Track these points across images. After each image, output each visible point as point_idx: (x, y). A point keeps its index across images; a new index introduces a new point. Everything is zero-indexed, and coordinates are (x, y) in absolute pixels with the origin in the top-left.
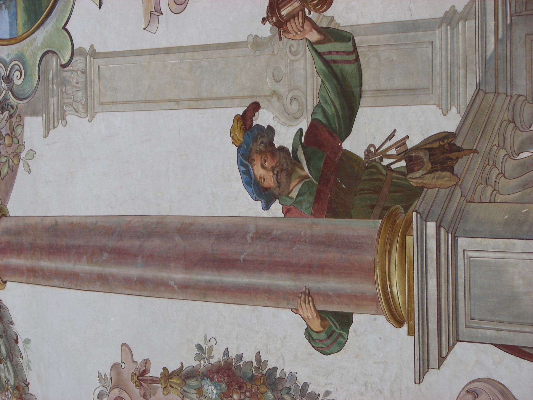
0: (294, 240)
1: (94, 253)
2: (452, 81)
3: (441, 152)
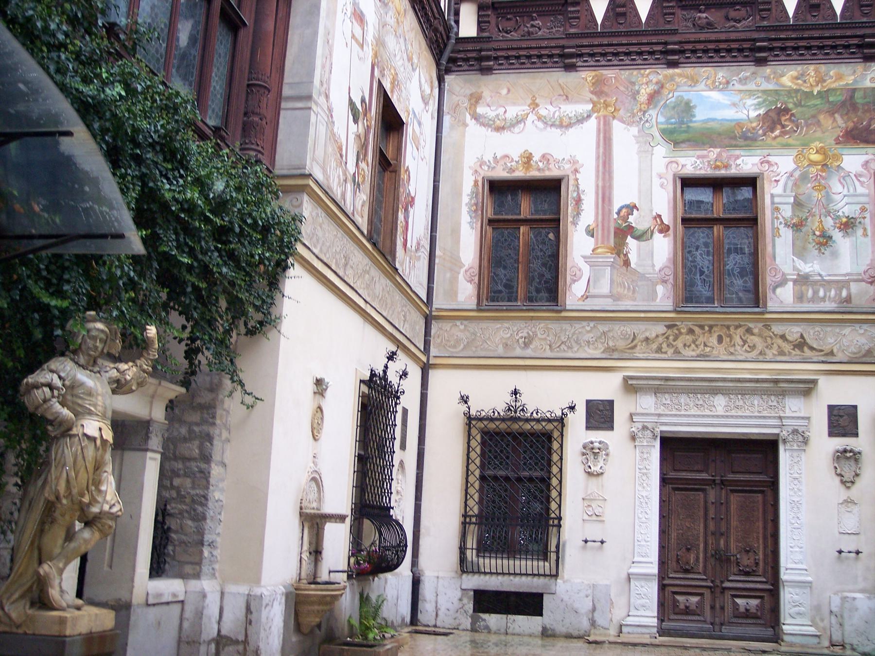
0: (609, 221)
1: (604, 154)
3: (627, 263)
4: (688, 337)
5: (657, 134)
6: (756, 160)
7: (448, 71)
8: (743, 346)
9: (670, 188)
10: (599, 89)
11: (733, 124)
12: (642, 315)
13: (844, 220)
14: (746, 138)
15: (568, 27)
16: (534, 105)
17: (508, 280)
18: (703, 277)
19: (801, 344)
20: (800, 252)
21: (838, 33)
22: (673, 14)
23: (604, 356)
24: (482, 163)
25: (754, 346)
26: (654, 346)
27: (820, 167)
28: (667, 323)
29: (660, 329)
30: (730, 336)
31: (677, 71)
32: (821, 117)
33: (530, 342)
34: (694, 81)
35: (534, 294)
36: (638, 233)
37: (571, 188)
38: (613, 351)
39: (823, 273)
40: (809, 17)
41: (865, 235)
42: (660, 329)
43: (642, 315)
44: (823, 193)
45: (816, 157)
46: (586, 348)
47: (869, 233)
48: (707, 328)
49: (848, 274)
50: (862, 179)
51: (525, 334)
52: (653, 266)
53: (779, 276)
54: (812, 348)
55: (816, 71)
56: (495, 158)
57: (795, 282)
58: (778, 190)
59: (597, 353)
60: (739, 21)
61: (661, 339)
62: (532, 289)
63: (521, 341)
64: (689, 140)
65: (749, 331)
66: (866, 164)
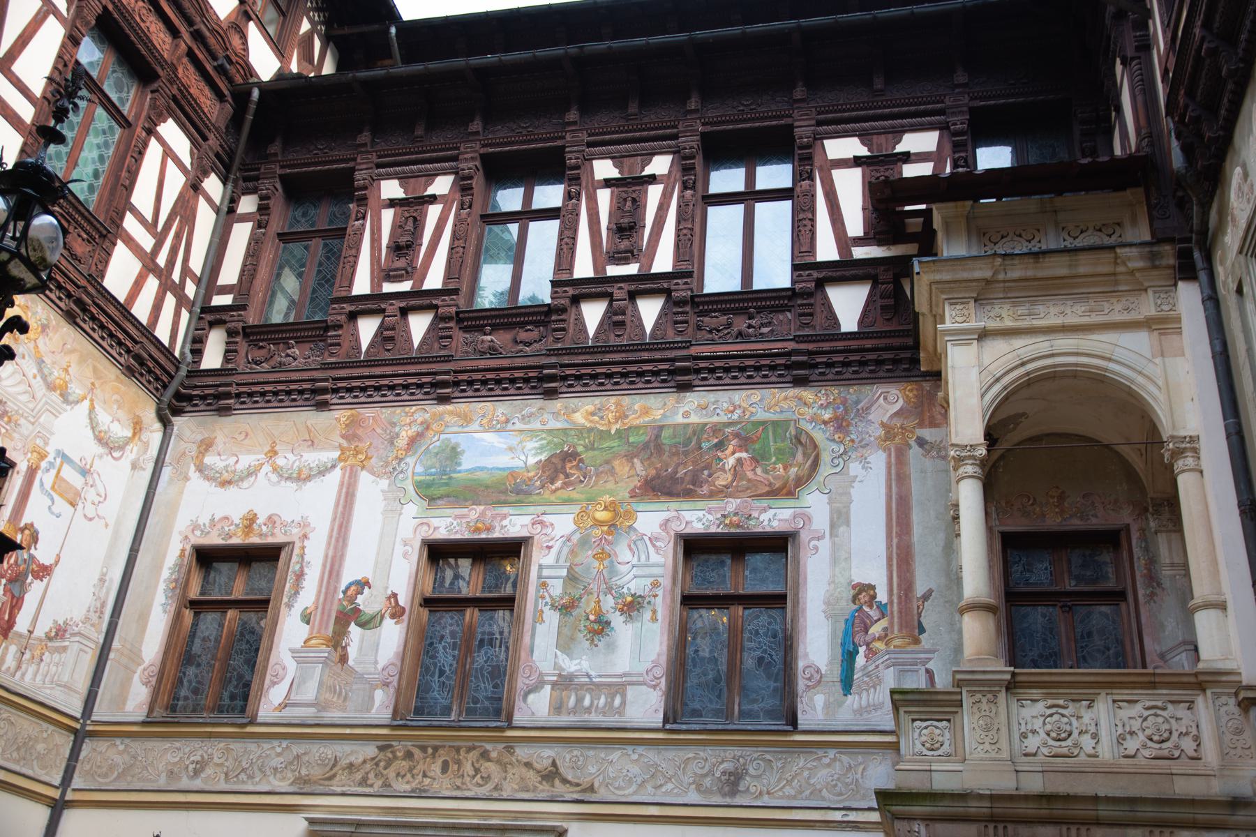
1: (343, 513)
2: (361, 663)
3: (344, 659)
4: (404, 763)
5: (410, 489)
6: (527, 520)
7: (177, 412)
8: (474, 777)
9: (415, 558)
10: (351, 433)
11: (506, 473)
12: (348, 731)
13: (629, 599)
14: (518, 492)
15: (326, 354)
16: (273, 453)
17: (199, 682)
18: (443, 679)
19: (552, 774)
20: (565, 643)
21: (645, 355)
22: (450, 337)
23: (291, 789)
24: (195, 527)
25: (489, 777)
26: (358, 776)
27: (606, 528)
28: (380, 743)
29: (370, 750)
30: (459, 763)
31: (449, 407)
32: (616, 463)
33: (203, 769)
34: (467, 419)
35: (227, 702)
36: (363, 619)
37: (294, 559)
38: (305, 782)
39: (593, 673)
40: (612, 336)
41: (654, 619)
42: (370, 750)
43: (348, 731)
44: (606, 562)
45: (602, 515)
46: (271, 778)
47: (659, 616)
48: (430, 751)
49: (625, 675)
50: (657, 544)
51: (198, 758)
52: (376, 662)
53: (535, 677)
54: (565, 781)
55: (618, 404)
56: (212, 520)
57: (554, 685)
58: (549, 559)
59: (283, 786)
60: (528, 344)
61: (368, 766)
62: (226, 694)
63: (191, 767)
64: (448, 496)
65: (485, 755)
66: (665, 524)
